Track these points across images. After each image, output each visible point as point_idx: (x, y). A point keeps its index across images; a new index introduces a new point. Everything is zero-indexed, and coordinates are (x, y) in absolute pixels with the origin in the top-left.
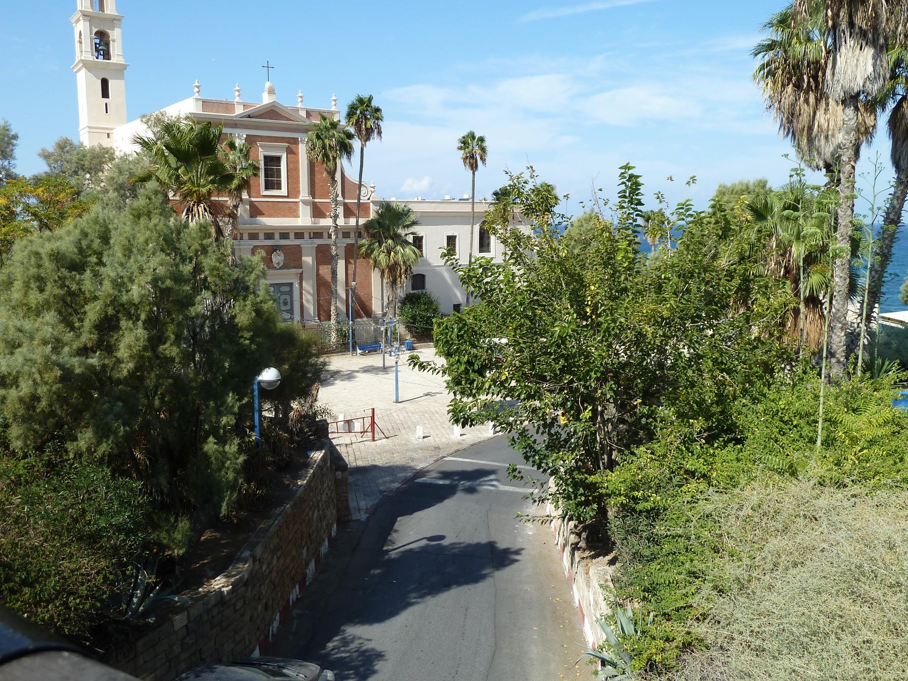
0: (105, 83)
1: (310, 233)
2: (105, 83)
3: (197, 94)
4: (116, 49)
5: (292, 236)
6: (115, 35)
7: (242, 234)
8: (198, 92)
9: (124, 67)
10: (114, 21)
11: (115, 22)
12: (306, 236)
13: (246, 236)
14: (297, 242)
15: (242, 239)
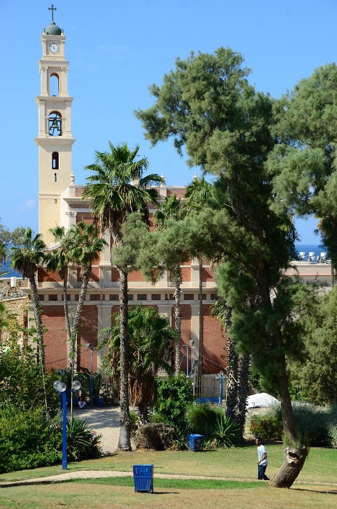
0: (55, 156)
1: (166, 295)
2: (55, 156)
3: (72, 183)
4: (66, 126)
5: (149, 297)
6: (66, 113)
7: (104, 296)
8: (73, 181)
9: (72, 142)
10: (66, 102)
11: (66, 103)
12: (163, 297)
13: (107, 297)
14: (155, 302)
15: (104, 299)
